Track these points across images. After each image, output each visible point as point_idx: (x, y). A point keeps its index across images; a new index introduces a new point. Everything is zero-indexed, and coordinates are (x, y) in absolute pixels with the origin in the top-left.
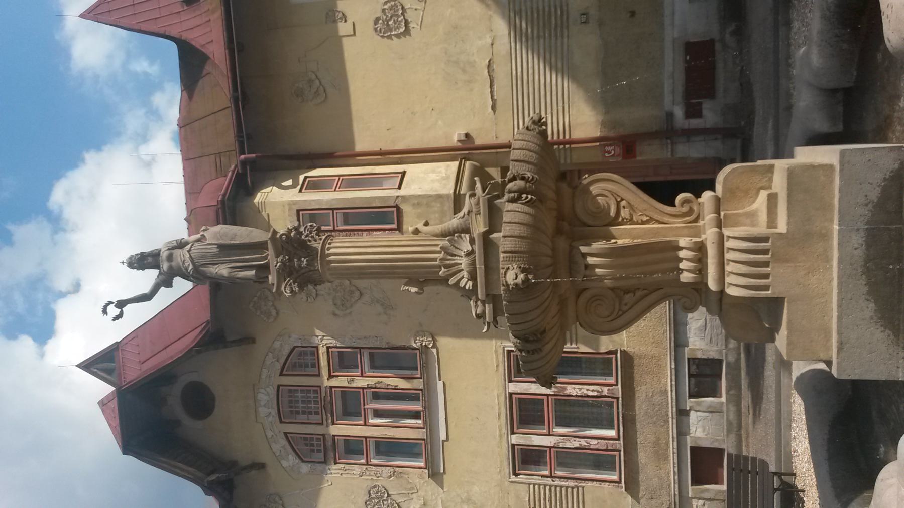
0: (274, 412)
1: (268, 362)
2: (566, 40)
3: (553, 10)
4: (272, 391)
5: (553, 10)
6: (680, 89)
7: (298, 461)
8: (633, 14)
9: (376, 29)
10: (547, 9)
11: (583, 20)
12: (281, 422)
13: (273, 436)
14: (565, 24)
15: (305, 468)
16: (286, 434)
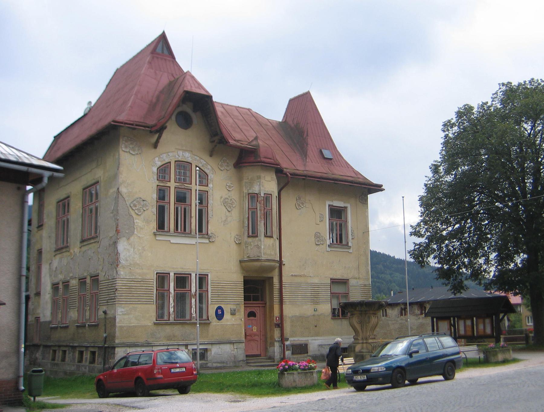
0: (180, 159)
1: (202, 160)
2: (310, 303)
3: (318, 299)
4: (189, 160)
5: (318, 299)
6: (295, 343)
7: (158, 166)
8: (316, 326)
9: (317, 233)
10: (319, 297)
11: (315, 310)
12: (175, 161)
13: (169, 155)
14: (314, 303)
15: (155, 169)
16: (170, 162)
